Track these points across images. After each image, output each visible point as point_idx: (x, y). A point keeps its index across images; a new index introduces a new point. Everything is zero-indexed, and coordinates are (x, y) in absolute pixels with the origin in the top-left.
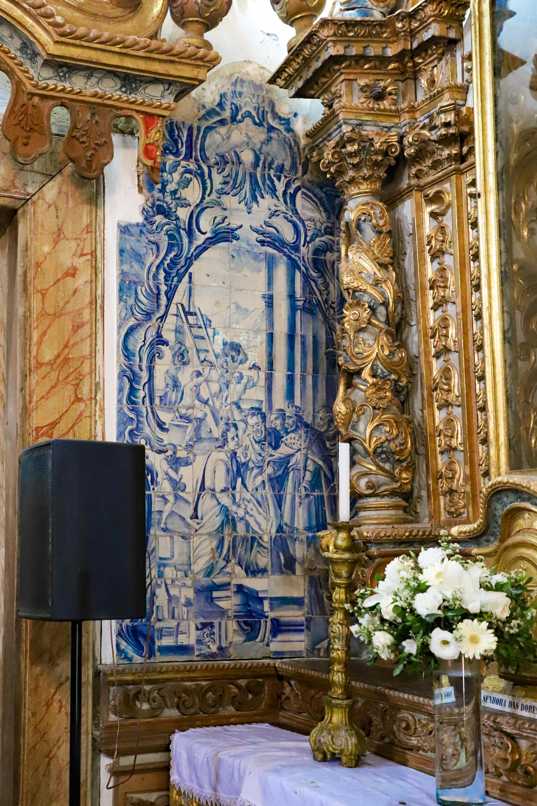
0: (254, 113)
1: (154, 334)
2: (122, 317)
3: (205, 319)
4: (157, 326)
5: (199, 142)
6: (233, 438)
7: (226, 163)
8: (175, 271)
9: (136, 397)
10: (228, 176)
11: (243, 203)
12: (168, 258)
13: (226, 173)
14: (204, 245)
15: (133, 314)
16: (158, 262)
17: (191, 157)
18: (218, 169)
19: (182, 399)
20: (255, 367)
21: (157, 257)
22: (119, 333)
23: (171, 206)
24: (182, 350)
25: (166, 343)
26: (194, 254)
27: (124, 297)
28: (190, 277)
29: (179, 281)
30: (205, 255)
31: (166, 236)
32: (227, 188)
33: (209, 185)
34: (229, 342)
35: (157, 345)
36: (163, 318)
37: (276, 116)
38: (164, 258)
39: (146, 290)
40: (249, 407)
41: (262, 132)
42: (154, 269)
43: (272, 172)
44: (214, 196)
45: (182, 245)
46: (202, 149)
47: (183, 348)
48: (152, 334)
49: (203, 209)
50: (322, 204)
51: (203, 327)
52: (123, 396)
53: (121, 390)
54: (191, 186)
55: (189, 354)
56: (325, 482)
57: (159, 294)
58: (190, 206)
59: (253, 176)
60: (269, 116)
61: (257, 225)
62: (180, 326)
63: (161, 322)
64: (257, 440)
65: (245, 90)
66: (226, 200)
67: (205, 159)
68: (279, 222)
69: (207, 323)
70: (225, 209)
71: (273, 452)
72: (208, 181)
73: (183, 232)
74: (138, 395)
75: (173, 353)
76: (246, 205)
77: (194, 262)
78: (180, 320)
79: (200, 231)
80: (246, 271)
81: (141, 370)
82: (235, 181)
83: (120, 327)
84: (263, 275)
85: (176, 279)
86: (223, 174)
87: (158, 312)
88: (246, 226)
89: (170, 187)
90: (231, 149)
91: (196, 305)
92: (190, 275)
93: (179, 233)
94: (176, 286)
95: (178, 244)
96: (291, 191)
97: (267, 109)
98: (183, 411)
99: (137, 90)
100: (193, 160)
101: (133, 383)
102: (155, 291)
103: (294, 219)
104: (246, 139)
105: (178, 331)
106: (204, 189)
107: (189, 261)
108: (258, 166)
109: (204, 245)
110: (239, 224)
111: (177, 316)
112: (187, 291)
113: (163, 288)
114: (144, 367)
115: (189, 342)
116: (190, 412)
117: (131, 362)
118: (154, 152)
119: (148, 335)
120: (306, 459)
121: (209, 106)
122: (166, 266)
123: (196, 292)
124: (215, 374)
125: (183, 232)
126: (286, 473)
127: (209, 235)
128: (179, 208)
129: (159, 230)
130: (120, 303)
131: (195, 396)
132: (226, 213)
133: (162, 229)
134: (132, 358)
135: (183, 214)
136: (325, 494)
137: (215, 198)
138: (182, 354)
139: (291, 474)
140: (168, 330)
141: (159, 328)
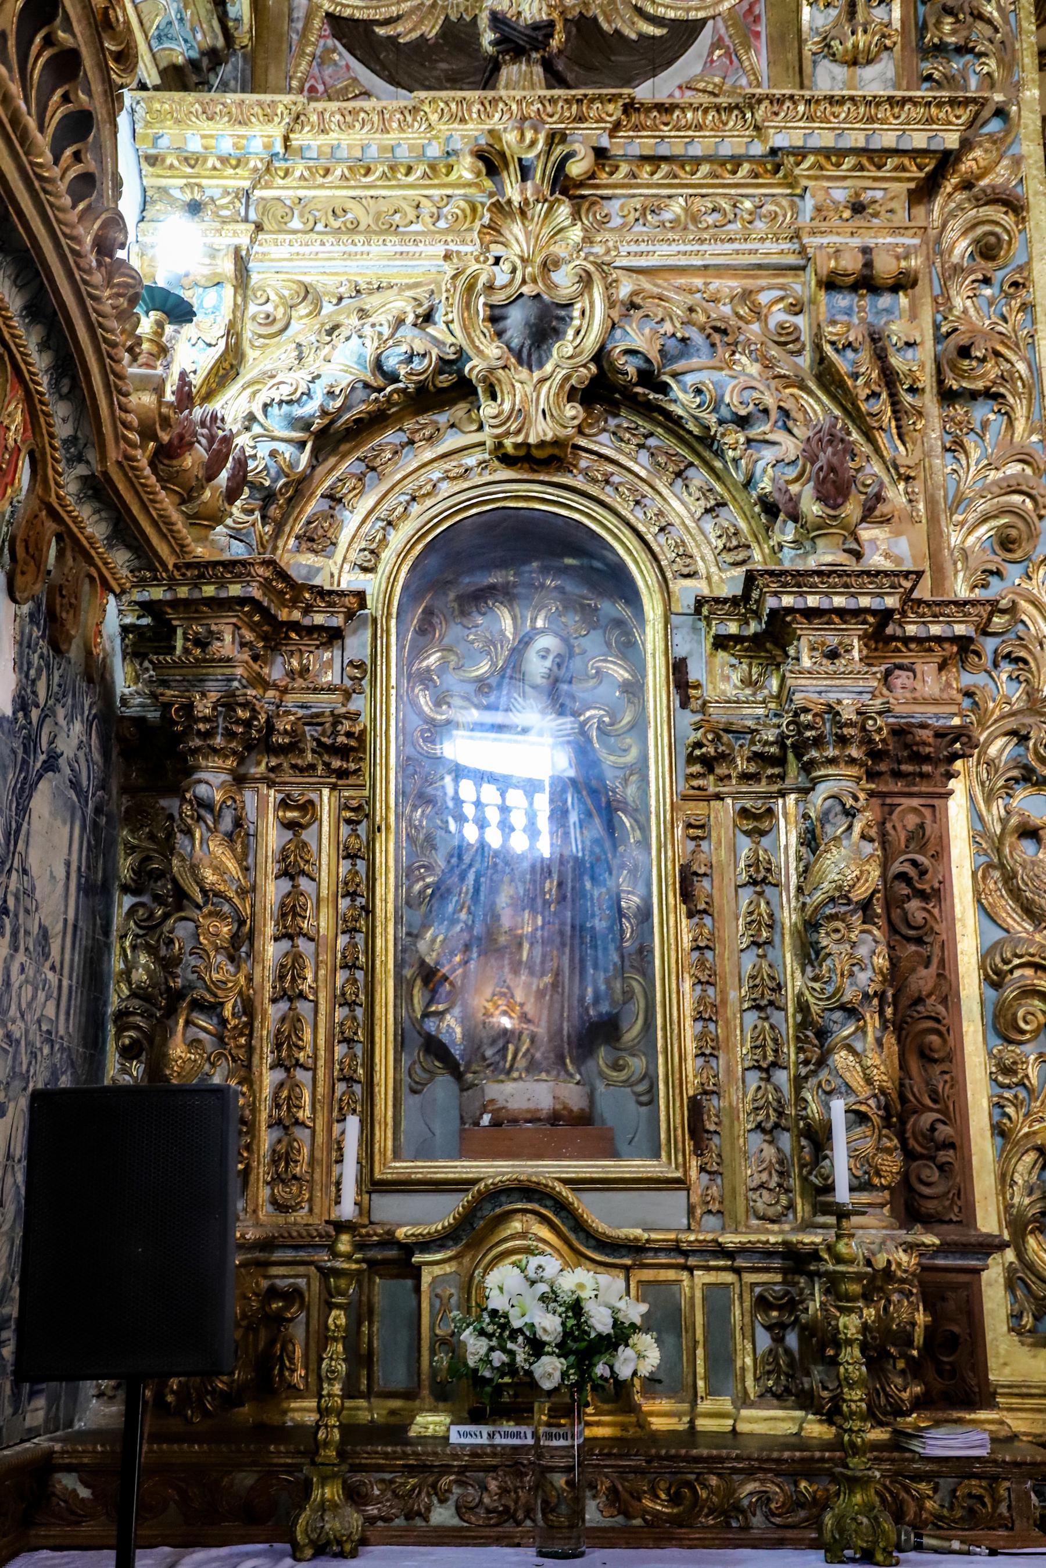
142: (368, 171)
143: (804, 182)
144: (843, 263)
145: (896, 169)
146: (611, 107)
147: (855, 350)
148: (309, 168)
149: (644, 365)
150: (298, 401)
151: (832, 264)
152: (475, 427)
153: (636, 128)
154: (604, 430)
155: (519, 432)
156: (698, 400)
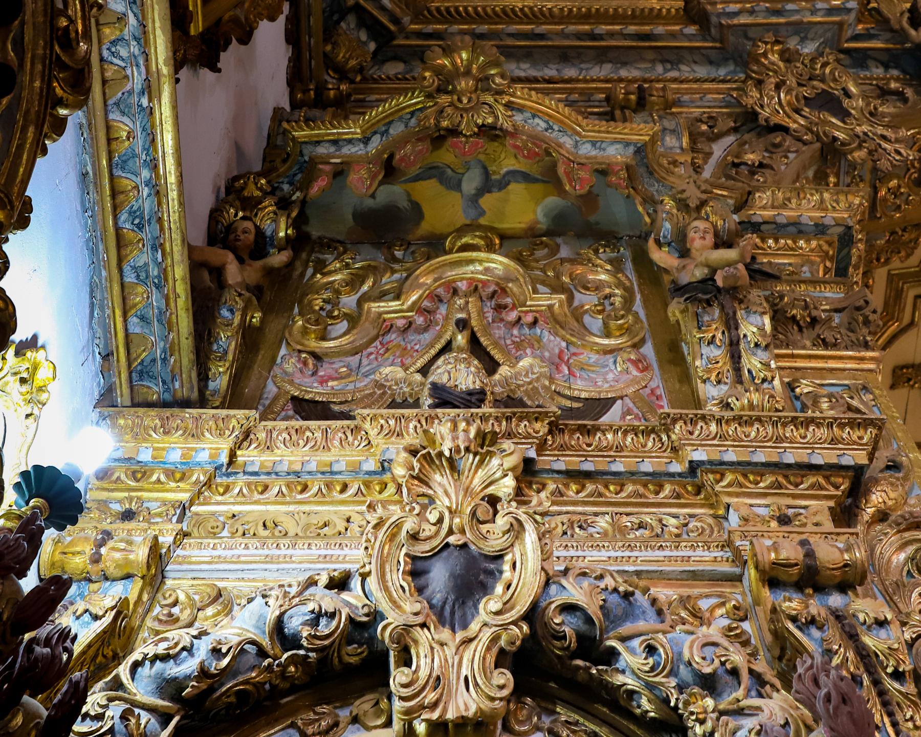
142: (305, 488)
143: (726, 499)
144: (783, 555)
145: (812, 487)
146: (537, 426)
147: (820, 628)
148: (249, 485)
149: (583, 627)
151: (773, 555)
153: (562, 447)
155: (434, 706)
156: (651, 661)
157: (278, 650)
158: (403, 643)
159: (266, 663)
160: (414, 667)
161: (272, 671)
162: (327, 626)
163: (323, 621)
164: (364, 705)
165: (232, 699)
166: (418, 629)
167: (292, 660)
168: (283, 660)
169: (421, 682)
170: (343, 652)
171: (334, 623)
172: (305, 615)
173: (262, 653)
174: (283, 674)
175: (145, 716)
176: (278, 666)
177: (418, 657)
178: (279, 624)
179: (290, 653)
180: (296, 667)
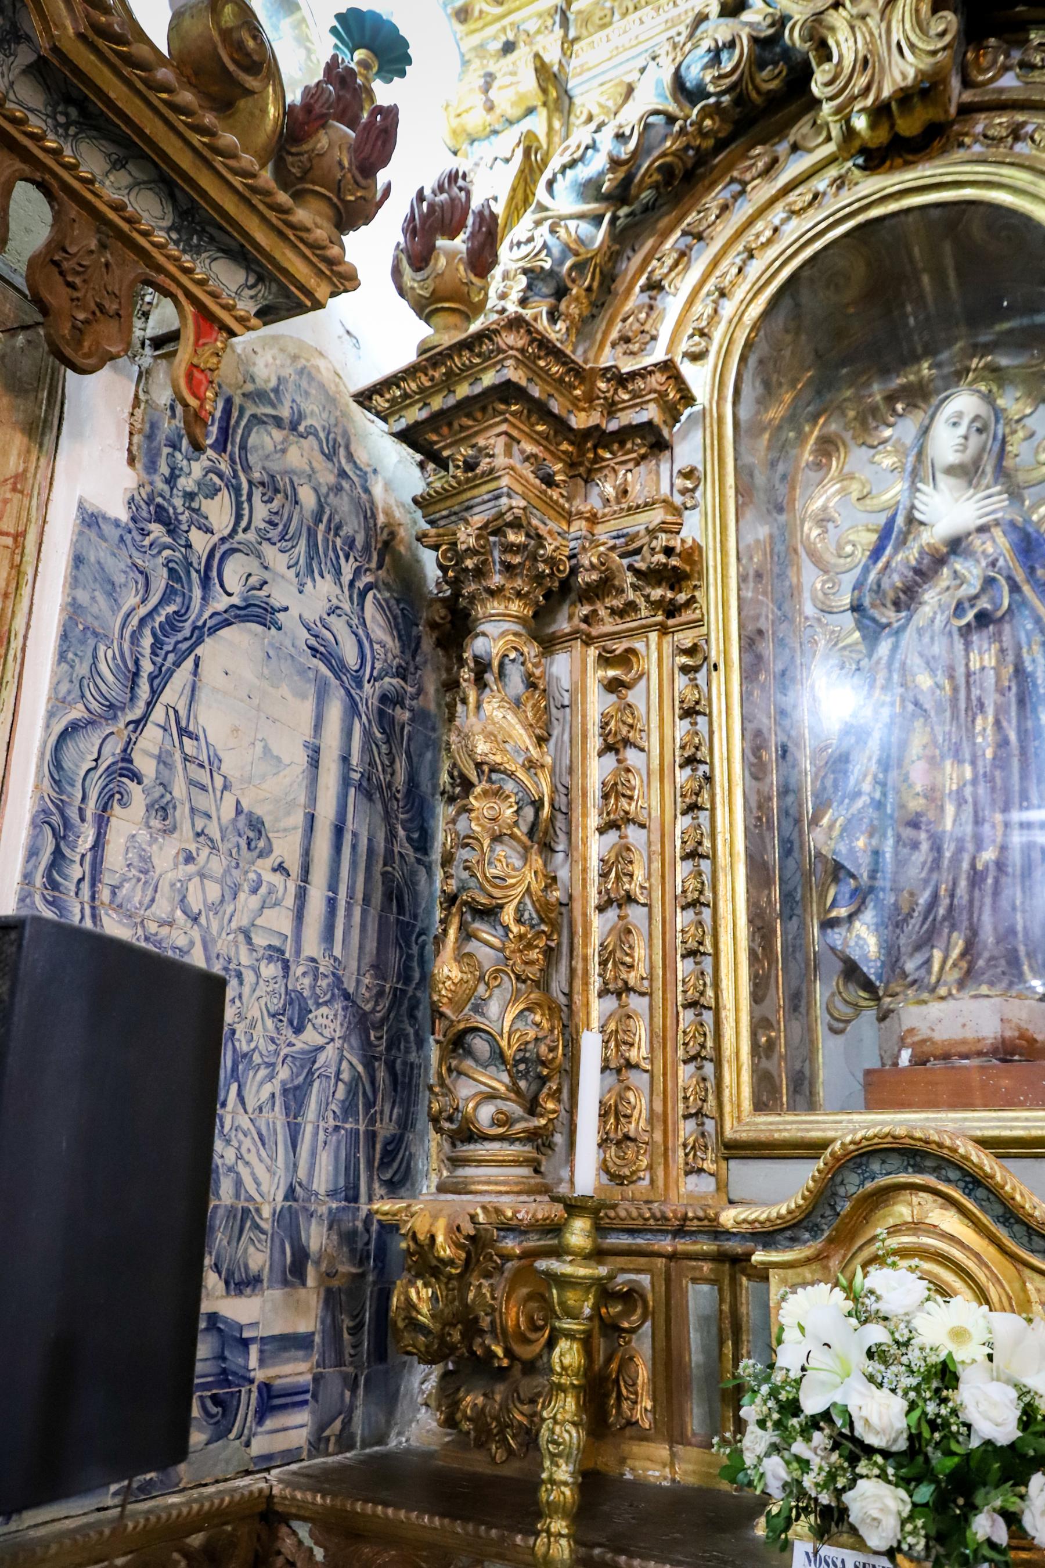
0: (322, 435)
1: (118, 751)
2: (61, 696)
3: (212, 754)
4: (126, 739)
5: (240, 431)
6: (233, 1001)
7: (277, 491)
8: (172, 641)
9: (65, 877)
10: (276, 513)
11: (293, 570)
12: (164, 613)
13: (275, 505)
14: (226, 616)
15: (83, 696)
16: (143, 611)
17: (225, 451)
18: (263, 494)
19: (153, 900)
20: (280, 868)
21: (143, 601)
22: (48, 726)
23: (180, 517)
24: (165, 800)
25: (136, 777)
26: (208, 625)
27: (70, 655)
28: (197, 665)
29: (177, 664)
30: (224, 632)
31: (165, 570)
32: (274, 534)
33: (246, 512)
34: (246, 810)
35: (121, 775)
36: (139, 724)
37: (350, 457)
38: (155, 610)
39: (114, 658)
40: (265, 943)
41: (331, 472)
42: (135, 622)
43: (338, 541)
44: (251, 536)
45: (191, 598)
46: (243, 447)
47: (168, 797)
48: (113, 749)
49: (234, 551)
50: (397, 625)
51: (206, 764)
52: (36, 867)
53: (33, 853)
54: (218, 498)
55: (178, 813)
56: (364, 1105)
57: (136, 674)
58: (212, 533)
59: (312, 534)
60: (342, 452)
61: (311, 617)
62: (167, 752)
63: (134, 731)
64: (272, 1010)
65: (313, 392)
66: (270, 552)
67: (247, 468)
68: (338, 625)
69: (213, 763)
70: (266, 568)
71: (293, 1038)
72: (246, 505)
73: (194, 575)
74: (67, 871)
75: (148, 801)
76: (297, 575)
77: (207, 640)
78: (168, 738)
79: (222, 586)
80: (285, 690)
81: (83, 820)
82: (286, 527)
83: (51, 715)
84: (307, 709)
85: (171, 657)
86: (269, 505)
87: (131, 709)
88: (294, 612)
89: (186, 483)
90: (286, 472)
91: (201, 721)
92: (197, 660)
93: (188, 573)
94: (171, 673)
95: (184, 594)
96: (360, 584)
97: (339, 439)
98: (153, 927)
99: (199, 253)
100: (226, 457)
101: (62, 844)
102: (131, 665)
103: (360, 632)
104: (307, 468)
105: (163, 760)
106: (239, 517)
107: (200, 634)
108: (321, 521)
109: (226, 616)
110: (285, 604)
111: (165, 730)
112: (188, 688)
113: (147, 667)
114: (89, 814)
115: (179, 789)
116: (164, 931)
117: (64, 797)
118: (203, 388)
119: (107, 750)
120: (342, 1058)
121: (260, 383)
122: (157, 625)
123: (203, 695)
124: (217, 865)
125: (194, 575)
126: (309, 1082)
127: (235, 600)
128: (193, 528)
129: (154, 552)
130: (59, 663)
131: (178, 898)
132: (267, 576)
133: (160, 552)
134: (69, 788)
135: (200, 542)
136: (362, 1128)
137: (253, 540)
138: (164, 809)
139: (316, 1084)
140: (146, 753)
141: (128, 743)
150: (582, 159)
152: (824, 134)
154: (1006, 68)
157: (687, 110)
158: (816, 38)
159: (677, 128)
160: (835, 59)
161: (687, 134)
162: (730, 59)
163: (724, 56)
164: (800, 130)
165: (657, 177)
166: (831, 11)
167: (705, 113)
168: (694, 117)
169: (847, 71)
170: (758, 81)
171: (737, 52)
172: (703, 57)
173: (671, 119)
174: (702, 134)
175: (572, 224)
176: (691, 125)
177: (838, 44)
178: (678, 80)
179: (699, 106)
180: (712, 119)
